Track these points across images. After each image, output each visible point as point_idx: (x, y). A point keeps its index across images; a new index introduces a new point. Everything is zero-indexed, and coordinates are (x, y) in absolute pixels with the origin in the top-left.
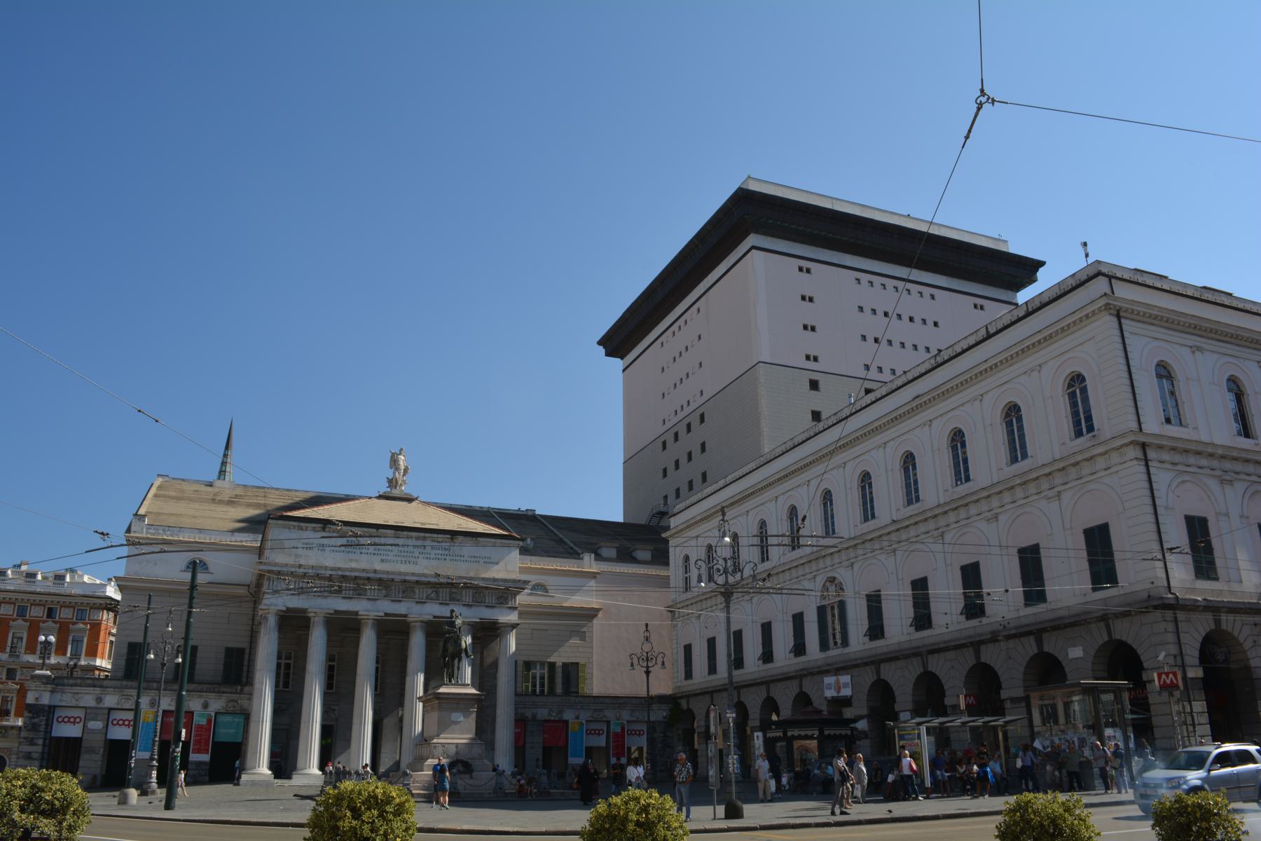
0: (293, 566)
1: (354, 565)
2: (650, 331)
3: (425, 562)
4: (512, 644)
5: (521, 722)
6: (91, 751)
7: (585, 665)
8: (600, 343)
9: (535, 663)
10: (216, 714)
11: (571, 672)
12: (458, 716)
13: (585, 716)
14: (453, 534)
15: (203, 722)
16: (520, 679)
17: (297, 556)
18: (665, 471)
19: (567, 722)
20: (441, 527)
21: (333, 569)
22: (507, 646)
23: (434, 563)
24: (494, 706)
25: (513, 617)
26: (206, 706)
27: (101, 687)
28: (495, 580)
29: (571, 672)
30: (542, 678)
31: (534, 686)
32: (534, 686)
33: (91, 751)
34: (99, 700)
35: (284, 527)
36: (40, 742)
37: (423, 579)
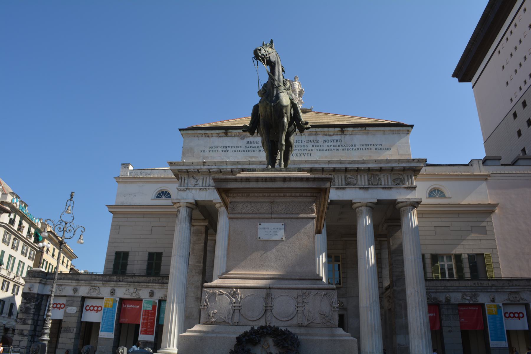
0: (198, 164)
1: (254, 160)
2: (488, 50)
3: (319, 153)
4: (414, 219)
5: (434, 307)
6: (68, 330)
7: (489, 256)
8: (454, 76)
9: (442, 256)
10: (160, 301)
11: (477, 262)
12: (272, 230)
13: (501, 299)
14: (343, 127)
15: (150, 308)
16: (429, 270)
17: (204, 158)
18: (519, 133)
19: (482, 305)
20: (331, 123)
21: (233, 163)
22: (410, 223)
23: (327, 153)
24: (404, 291)
25: (411, 196)
26: (152, 294)
27: (78, 280)
28: (388, 161)
29: (477, 262)
30: (450, 269)
31: (443, 274)
32: (443, 274)
33: (68, 330)
34: (75, 290)
35: (194, 136)
36: (30, 322)
37: (316, 166)
